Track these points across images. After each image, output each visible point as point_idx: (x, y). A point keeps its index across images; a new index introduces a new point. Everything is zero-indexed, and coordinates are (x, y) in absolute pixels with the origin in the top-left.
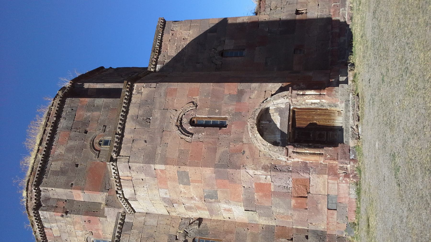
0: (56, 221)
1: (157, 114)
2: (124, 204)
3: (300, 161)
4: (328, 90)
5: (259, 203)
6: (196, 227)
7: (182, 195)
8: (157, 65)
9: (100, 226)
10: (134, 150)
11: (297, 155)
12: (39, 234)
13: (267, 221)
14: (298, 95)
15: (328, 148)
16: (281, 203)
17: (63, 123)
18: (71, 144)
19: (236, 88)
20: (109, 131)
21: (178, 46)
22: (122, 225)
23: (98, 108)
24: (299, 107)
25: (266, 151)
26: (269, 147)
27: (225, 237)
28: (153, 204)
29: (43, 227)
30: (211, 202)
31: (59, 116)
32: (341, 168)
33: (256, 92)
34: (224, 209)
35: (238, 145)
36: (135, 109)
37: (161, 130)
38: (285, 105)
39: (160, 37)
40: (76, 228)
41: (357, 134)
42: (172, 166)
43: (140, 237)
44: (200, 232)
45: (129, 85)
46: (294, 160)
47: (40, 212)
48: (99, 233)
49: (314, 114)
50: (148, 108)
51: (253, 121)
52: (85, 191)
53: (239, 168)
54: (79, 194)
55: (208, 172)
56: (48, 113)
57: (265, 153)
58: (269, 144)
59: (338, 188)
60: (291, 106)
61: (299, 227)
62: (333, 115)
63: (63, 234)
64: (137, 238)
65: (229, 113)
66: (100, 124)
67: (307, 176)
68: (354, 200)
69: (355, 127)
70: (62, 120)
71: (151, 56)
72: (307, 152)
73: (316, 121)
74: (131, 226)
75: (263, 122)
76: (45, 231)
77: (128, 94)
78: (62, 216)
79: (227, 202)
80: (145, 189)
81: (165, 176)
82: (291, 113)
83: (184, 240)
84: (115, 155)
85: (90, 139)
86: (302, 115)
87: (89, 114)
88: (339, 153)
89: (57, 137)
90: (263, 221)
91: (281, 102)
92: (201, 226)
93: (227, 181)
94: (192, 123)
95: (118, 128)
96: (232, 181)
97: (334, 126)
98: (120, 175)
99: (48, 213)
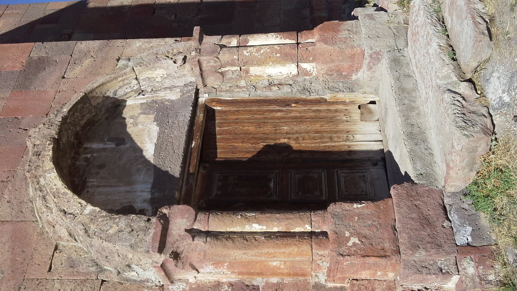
3: (224, 280)
4: (321, 29)
11: (207, 247)
14: (221, 48)
15: (346, 206)
19: (26, 56)
24: (226, 97)
25: (80, 245)
26: (87, 221)
33: (87, 62)
38: (181, 91)
41: (484, 111)
46: (200, 277)
49: (279, 118)
57: (74, 256)
58: (90, 208)
60: (200, 95)
62: (345, 118)
72: (256, 227)
73: (289, 138)
82: (201, 116)
86: (237, 123)
88: (398, 225)
91: (168, 83)
97: (351, 152)
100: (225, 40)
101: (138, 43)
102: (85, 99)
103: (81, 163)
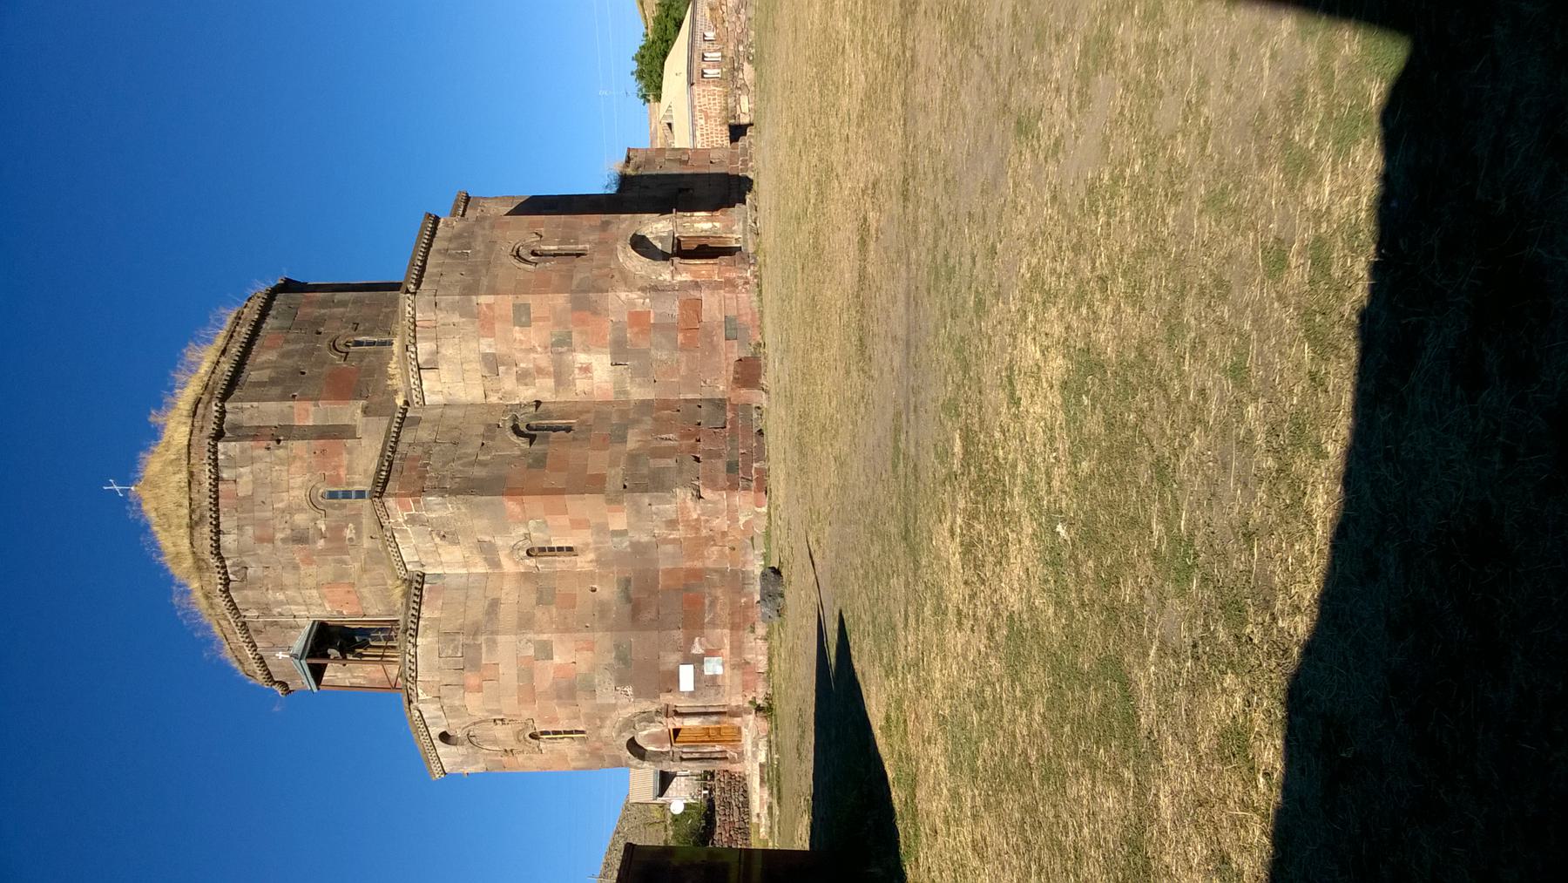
0: (253, 460)
1: (479, 246)
2: (413, 377)
6: (534, 409)
7: (517, 345)
9: (345, 457)
10: (442, 282)
12: (207, 491)
13: (643, 390)
16: (663, 341)
17: (269, 323)
20: (364, 330)
22: (403, 419)
23: (343, 304)
28: (464, 371)
29: (217, 479)
30: (560, 353)
31: (264, 313)
32: (739, 277)
34: (580, 365)
36: (443, 242)
39: (461, 212)
40: (293, 469)
42: (506, 296)
43: (434, 431)
44: (536, 417)
47: (220, 445)
48: (338, 475)
52: (320, 403)
53: (607, 291)
54: (307, 411)
55: (561, 300)
56: (236, 318)
59: (737, 301)
61: (689, 396)
63: (260, 490)
65: (590, 243)
66: (346, 322)
67: (696, 294)
68: (757, 310)
69: (753, 225)
70: (269, 320)
74: (417, 421)
76: (220, 487)
77: (430, 226)
78: (269, 449)
79: (587, 350)
80: (457, 340)
82: (676, 241)
83: (512, 425)
84: (412, 286)
87: (323, 311)
90: (638, 393)
92: (539, 409)
93: (588, 313)
94: (534, 253)
98: (417, 319)
99: (238, 444)
100: (685, 214)
101: (647, 215)
102: (635, 234)
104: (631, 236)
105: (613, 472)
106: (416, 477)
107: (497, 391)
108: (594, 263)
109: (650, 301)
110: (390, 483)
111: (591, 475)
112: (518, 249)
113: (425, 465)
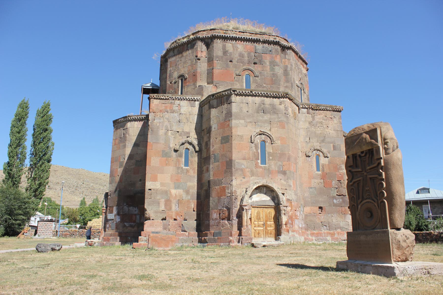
1: (267, 117)
5: (214, 189)
8: (306, 109)
10: (241, 105)
17: (260, 47)
18: (245, 54)
20: (256, 80)
21: (322, 123)
23: (272, 69)
27: (191, 168)
31: (264, 42)
33: (285, 183)
35: (248, 174)
37: (255, 121)
45: (286, 95)
50: (271, 110)
51: (265, 182)
58: (250, 194)
64: (186, 111)
66: (260, 73)
71: (313, 104)
75: (265, 189)
80: (217, 114)
81: (226, 127)
85: (250, 68)
87: (268, 64)
89: (249, 44)
95: (255, 92)
96: (226, 172)
103: (261, 188)
104: (269, 185)
105: (158, 184)
106: (161, 109)
107: (204, 134)
108: (254, 169)
109: (230, 196)
110: (159, 100)
111: (157, 175)
112: (263, 134)
113: (168, 112)
